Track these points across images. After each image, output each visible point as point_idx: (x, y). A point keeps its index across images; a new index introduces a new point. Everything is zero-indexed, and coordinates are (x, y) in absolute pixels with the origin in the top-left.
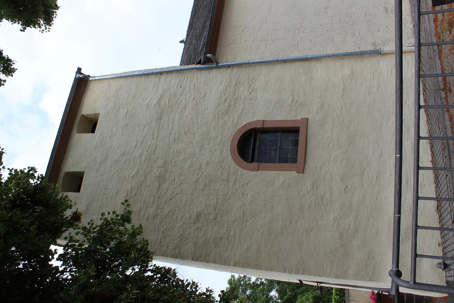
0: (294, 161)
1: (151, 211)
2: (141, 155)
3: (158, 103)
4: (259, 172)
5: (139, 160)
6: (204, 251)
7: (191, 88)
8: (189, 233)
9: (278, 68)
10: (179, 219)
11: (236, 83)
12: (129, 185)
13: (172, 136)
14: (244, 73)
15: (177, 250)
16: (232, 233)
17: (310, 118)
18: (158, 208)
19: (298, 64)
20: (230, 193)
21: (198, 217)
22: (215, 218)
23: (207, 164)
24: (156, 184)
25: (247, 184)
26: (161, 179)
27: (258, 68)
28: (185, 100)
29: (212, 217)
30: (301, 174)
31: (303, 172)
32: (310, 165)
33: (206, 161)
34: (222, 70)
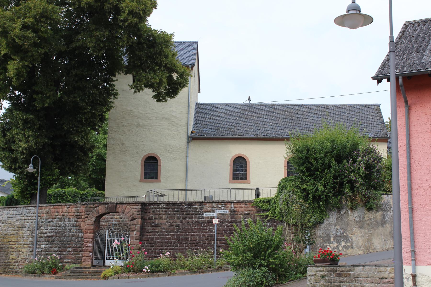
0: (145, 178)
1: (125, 124)
2: (148, 113)
3: (173, 116)
4: (140, 166)
5: (146, 113)
6: (111, 148)
7: (179, 131)
8: (117, 142)
9: (184, 169)
10: (122, 136)
11: (179, 152)
12: (135, 111)
13: (157, 126)
14: (184, 155)
15: (111, 138)
16: (118, 158)
17: (161, 183)
18: (126, 126)
19: (185, 177)
20: (133, 155)
21: (123, 144)
22: (123, 151)
23: (144, 145)
24: (135, 123)
25: (136, 162)
26: (138, 125)
27: (185, 160)
28: (173, 129)
29: (123, 150)
30: (139, 181)
31: (140, 182)
32: (142, 184)
33: (145, 144)
34: (186, 144)
